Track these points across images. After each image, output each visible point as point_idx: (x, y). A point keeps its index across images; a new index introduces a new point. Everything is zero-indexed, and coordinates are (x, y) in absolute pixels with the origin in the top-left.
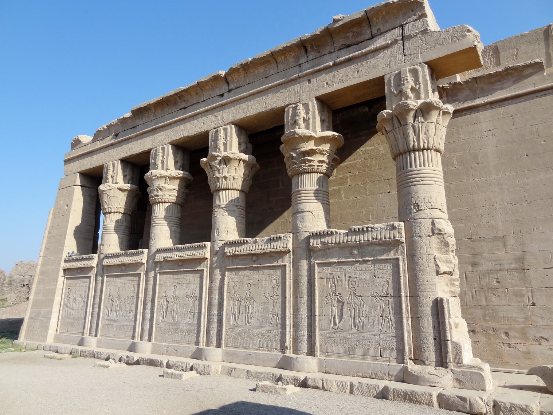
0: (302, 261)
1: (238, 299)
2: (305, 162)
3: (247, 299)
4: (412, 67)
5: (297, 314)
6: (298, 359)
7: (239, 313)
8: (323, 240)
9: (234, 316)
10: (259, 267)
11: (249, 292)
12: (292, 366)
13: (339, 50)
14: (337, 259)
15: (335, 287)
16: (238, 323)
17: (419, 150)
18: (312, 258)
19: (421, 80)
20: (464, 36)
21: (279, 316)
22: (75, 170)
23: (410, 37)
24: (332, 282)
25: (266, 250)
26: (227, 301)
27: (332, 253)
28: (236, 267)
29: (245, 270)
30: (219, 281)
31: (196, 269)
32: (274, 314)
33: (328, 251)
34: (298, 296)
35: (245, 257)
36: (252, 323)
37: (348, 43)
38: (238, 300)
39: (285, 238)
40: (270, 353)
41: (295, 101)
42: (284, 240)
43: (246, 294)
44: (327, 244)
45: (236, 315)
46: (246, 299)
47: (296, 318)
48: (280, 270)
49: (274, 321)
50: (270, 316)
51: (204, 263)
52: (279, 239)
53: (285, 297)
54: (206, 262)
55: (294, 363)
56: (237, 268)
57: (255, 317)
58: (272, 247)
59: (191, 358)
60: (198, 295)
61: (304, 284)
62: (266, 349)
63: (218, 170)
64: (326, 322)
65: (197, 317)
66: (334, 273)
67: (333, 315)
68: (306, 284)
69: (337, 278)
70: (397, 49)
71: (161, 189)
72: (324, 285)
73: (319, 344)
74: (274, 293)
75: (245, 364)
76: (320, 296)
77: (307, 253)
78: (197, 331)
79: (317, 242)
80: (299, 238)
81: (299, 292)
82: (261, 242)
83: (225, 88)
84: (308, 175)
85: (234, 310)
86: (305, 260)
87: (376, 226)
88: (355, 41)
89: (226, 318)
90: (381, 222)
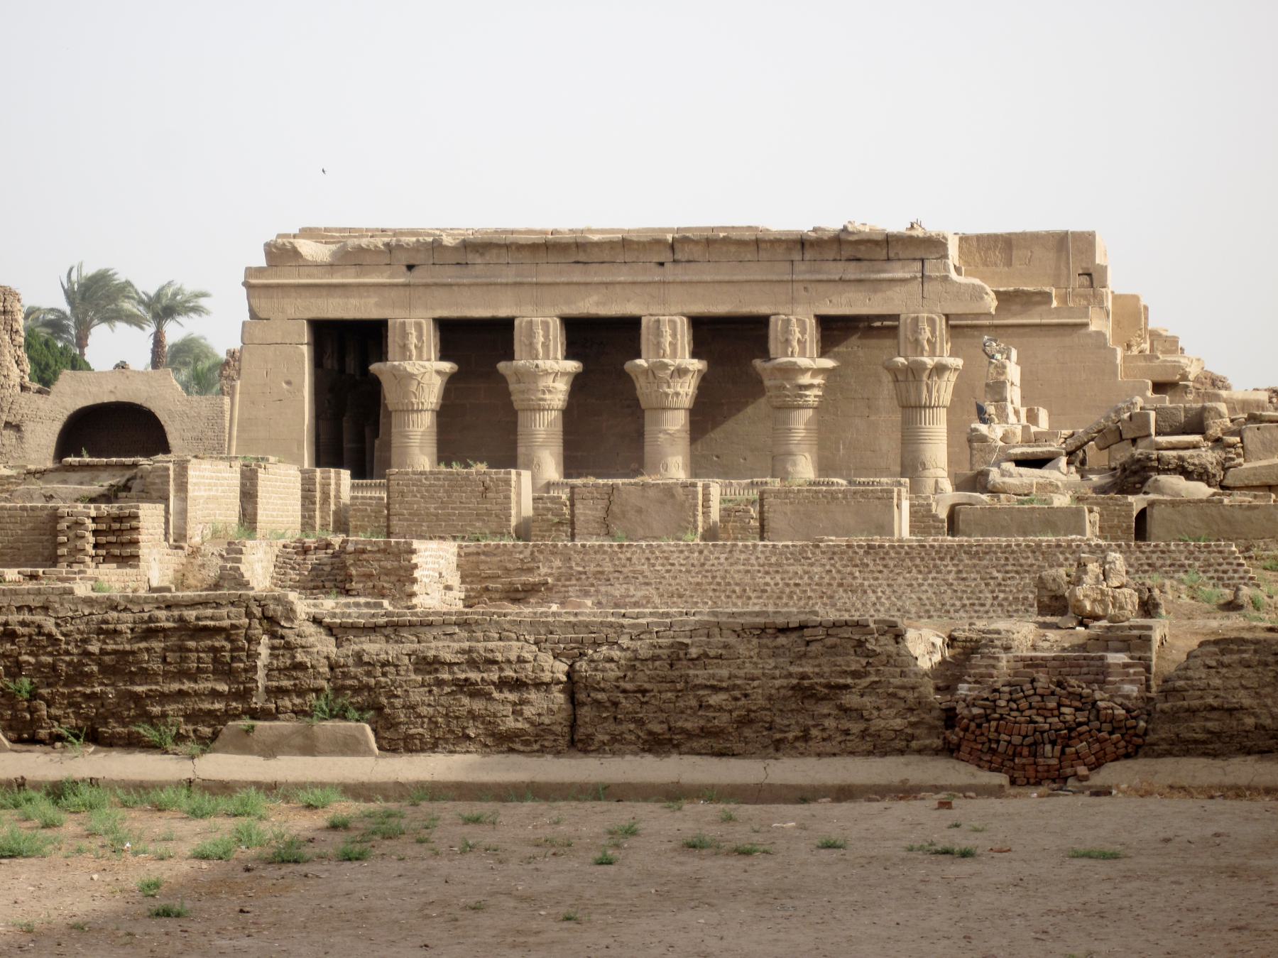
2: (801, 396)
4: (930, 315)
13: (849, 260)
17: (930, 407)
19: (938, 333)
20: (982, 298)
22: (291, 311)
23: (930, 277)
37: (859, 256)
41: (786, 311)
63: (668, 382)
70: (916, 286)
71: (550, 391)
83: (666, 256)
84: (802, 412)
87: (882, 480)
88: (867, 257)
90: (887, 477)
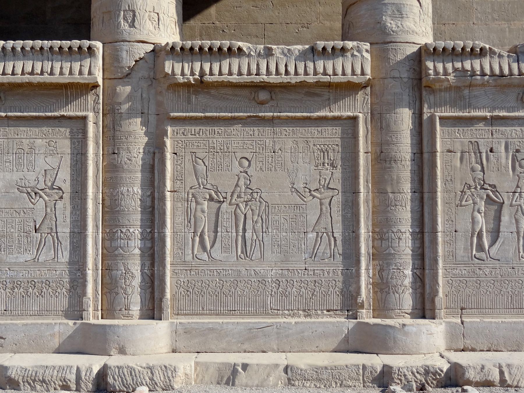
0: (398, 110)
1: (210, 195)
3: (239, 197)
5: (385, 230)
6: (406, 328)
7: (216, 232)
8: (458, 65)
9: (197, 239)
10: (279, 118)
12: (391, 344)
14: (489, 112)
15: (483, 170)
18: (426, 106)
21: (338, 235)
24: (473, 160)
25: (301, 78)
26: (174, 200)
27: (475, 96)
28: (230, 114)
29: (232, 125)
30: (141, 151)
31: (56, 114)
32: (323, 230)
33: (466, 92)
34: (389, 190)
35: (229, 91)
38: (211, 199)
39: (356, 53)
40: (313, 320)
42: (353, 55)
43: (237, 185)
44: (471, 76)
45: (206, 237)
46: (235, 196)
47: (382, 239)
48: (339, 130)
49: (322, 247)
50: (312, 236)
51: (86, 100)
52: (338, 52)
53: (356, 192)
54: (90, 98)
55: (394, 338)
56: (206, 118)
57: (265, 239)
58: (321, 71)
59: (58, 351)
60: (67, 187)
61: (403, 163)
62: (301, 312)
64: (461, 245)
65: (66, 243)
66: (481, 142)
67: (478, 230)
68: (409, 163)
69: (487, 152)
72: (455, 167)
73: (443, 293)
74: (323, 183)
75: (245, 352)
76: (446, 191)
77: (411, 94)
78: (72, 281)
79: (445, 68)
80: (391, 56)
81: (392, 180)
82: (285, 55)
85: (198, 224)
86: (407, 109)
89: (173, 244)
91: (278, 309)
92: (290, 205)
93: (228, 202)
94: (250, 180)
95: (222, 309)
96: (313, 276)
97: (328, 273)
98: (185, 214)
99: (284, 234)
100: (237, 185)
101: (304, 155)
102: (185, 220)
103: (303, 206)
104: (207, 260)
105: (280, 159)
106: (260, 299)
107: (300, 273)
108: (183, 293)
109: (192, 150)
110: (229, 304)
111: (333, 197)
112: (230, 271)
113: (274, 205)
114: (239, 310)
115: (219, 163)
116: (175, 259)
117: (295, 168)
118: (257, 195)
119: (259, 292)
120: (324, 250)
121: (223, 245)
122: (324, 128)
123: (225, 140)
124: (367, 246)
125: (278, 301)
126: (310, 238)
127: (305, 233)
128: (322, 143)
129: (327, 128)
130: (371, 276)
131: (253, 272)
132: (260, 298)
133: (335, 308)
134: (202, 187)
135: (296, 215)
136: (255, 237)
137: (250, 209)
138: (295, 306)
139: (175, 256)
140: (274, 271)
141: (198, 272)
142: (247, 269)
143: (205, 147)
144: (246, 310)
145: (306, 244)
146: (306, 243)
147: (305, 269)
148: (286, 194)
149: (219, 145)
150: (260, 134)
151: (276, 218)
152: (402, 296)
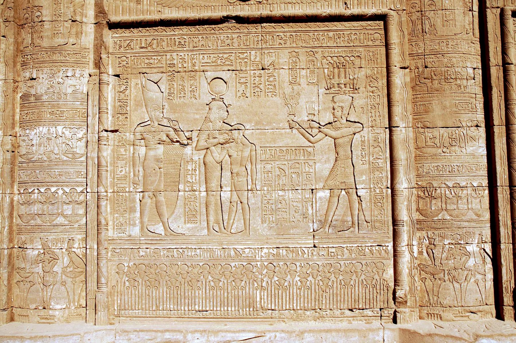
11: (219, 108)
16: (174, 226)
36: (238, 225)
46: (204, 136)
74: (338, 114)
91: (273, 308)
92: (289, 148)
93: (194, 145)
94: (228, 111)
95: (186, 309)
96: (327, 257)
97: (350, 251)
98: (129, 165)
99: (281, 193)
100: (207, 119)
101: (308, 73)
102: (130, 172)
103: (309, 149)
104: (163, 234)
105: (271, 79)
106: (244, 294)
107: (306, 252)
108: (127, 283)
109: (140, 70)
110: (197, 300)
111: (355, 134)
112: (198, 251)
113: (265, 149)
114: (213, 310)
115: (180, 87)
116: (116, 233)
117: (295, 92)
118: (239, 133)
119: (243, 282)
120: (343, 216)
121: (187, 210)
122: (337, 33)
123: (190, 54)
124: (409, 209)
125: (273, 296)
126: (320, 198)
127: (312, 190)
128: (336, 55)
129: (342, 32)
130: (416, 255)
131: (232, 253)
132: (244, 292)
133: (360, 306)
134: (156, 124)
135: (299, 163)
136: (235, 198)
137: (227, 156)
138: (298, 305)
139: (116, 228)
140: (265, 251)
141: (150, 252)
142: (224, 247)
143: (162, 66)
144: (222, 309)
145: (314, 208)
146: (314, 205)
147: (315, 246)
148: (283, 131)
149: (181, 61)
150: (242, 43)
151: (268, 167)
152: (464, 285)
